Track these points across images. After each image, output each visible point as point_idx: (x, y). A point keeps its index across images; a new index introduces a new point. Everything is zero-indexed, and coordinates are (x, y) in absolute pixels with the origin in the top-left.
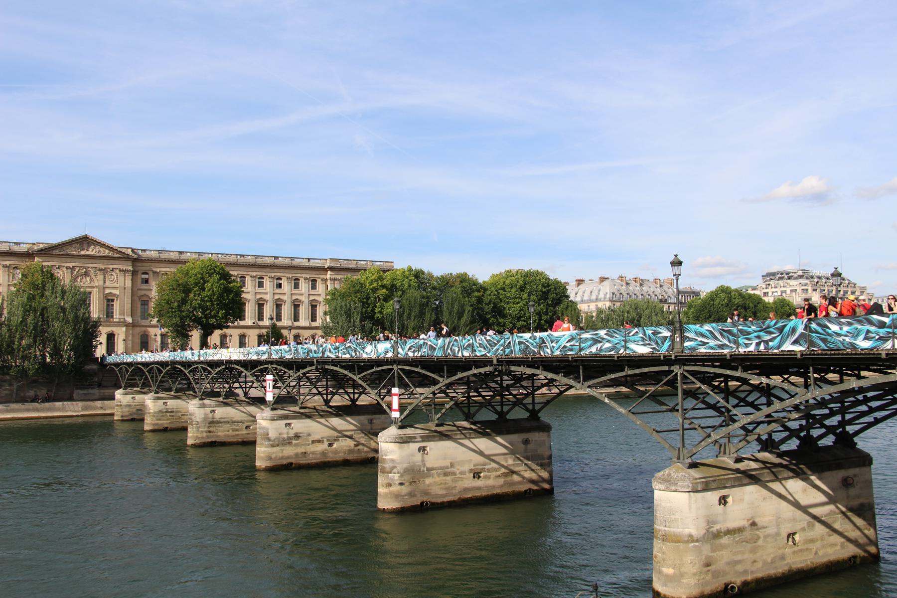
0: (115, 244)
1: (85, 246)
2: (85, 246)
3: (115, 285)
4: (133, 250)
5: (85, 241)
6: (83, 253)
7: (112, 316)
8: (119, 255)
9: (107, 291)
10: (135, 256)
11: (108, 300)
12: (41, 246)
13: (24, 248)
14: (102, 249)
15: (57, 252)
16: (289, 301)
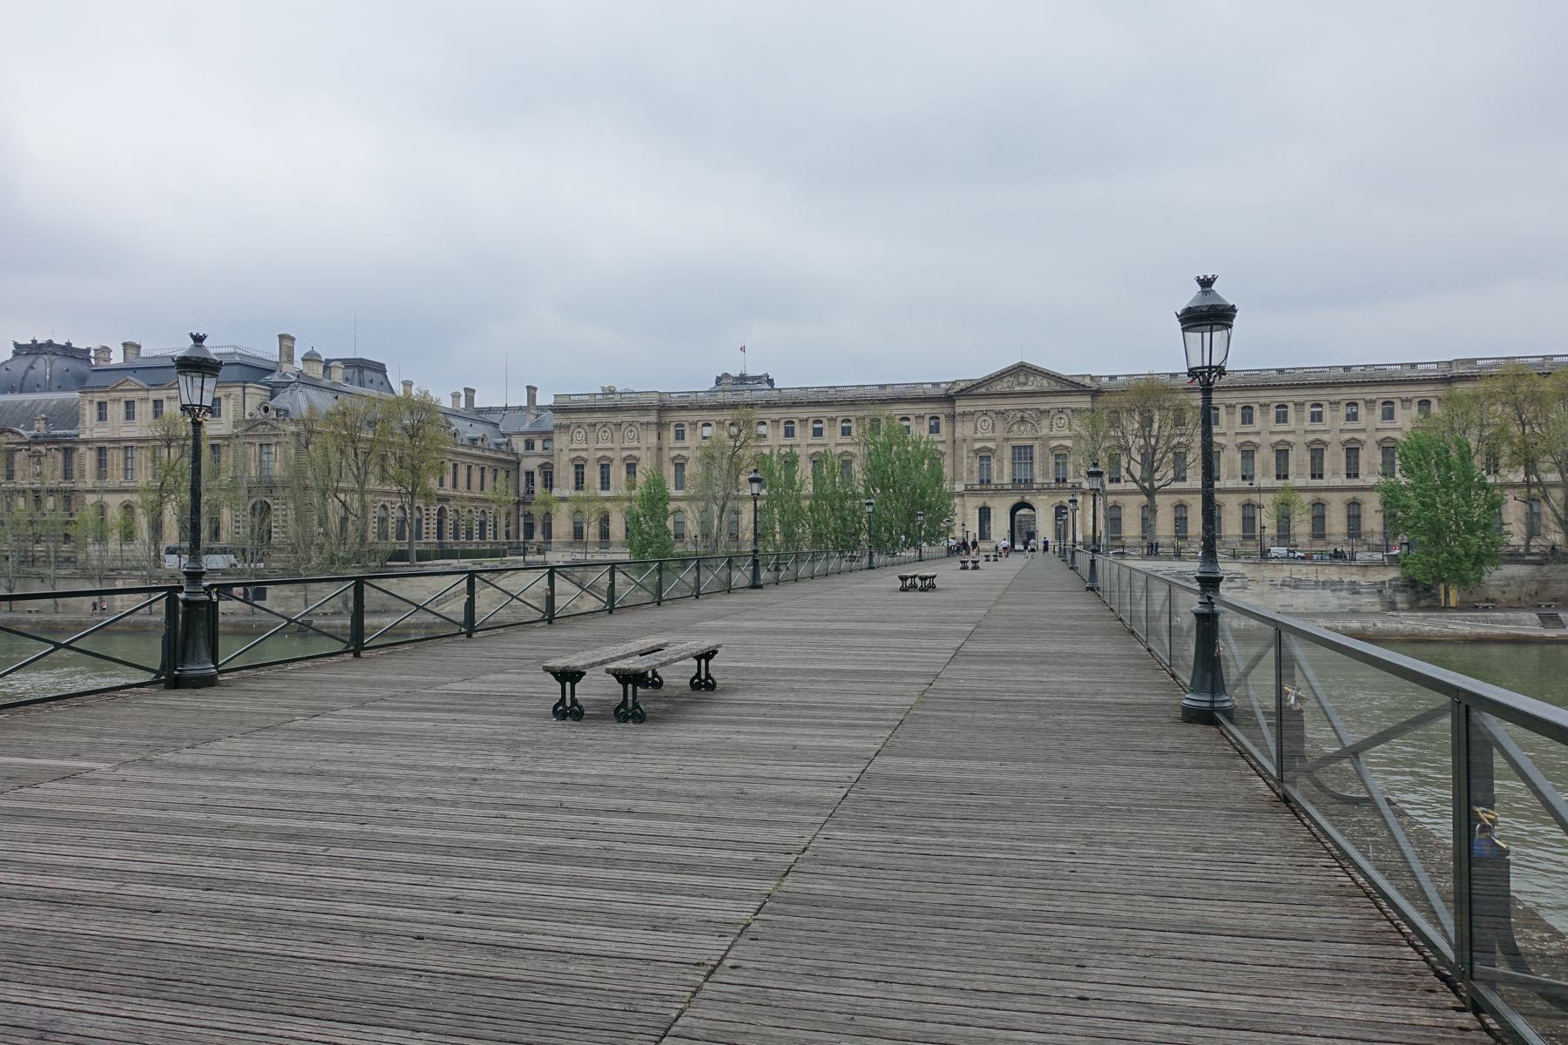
0: (1065, 371)
1: (1022, 379)
2: (1022, 379)
3: (1067, 432)
4: (1092, 378)
5: (1022, 370)
6: (1018, 389)
7: (1064, 480)
8: (1072, 386)
9: (1054, 443)
10: (1094, 386)
11: (1057, 456)
12: (962, 385)
13: (940, 391)
14: (1045, 382)
15: (983, 390)
16: (1371, 442)
